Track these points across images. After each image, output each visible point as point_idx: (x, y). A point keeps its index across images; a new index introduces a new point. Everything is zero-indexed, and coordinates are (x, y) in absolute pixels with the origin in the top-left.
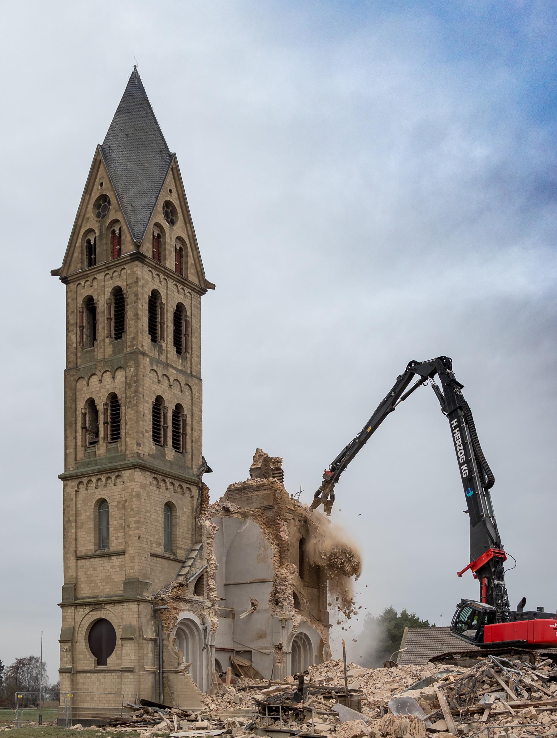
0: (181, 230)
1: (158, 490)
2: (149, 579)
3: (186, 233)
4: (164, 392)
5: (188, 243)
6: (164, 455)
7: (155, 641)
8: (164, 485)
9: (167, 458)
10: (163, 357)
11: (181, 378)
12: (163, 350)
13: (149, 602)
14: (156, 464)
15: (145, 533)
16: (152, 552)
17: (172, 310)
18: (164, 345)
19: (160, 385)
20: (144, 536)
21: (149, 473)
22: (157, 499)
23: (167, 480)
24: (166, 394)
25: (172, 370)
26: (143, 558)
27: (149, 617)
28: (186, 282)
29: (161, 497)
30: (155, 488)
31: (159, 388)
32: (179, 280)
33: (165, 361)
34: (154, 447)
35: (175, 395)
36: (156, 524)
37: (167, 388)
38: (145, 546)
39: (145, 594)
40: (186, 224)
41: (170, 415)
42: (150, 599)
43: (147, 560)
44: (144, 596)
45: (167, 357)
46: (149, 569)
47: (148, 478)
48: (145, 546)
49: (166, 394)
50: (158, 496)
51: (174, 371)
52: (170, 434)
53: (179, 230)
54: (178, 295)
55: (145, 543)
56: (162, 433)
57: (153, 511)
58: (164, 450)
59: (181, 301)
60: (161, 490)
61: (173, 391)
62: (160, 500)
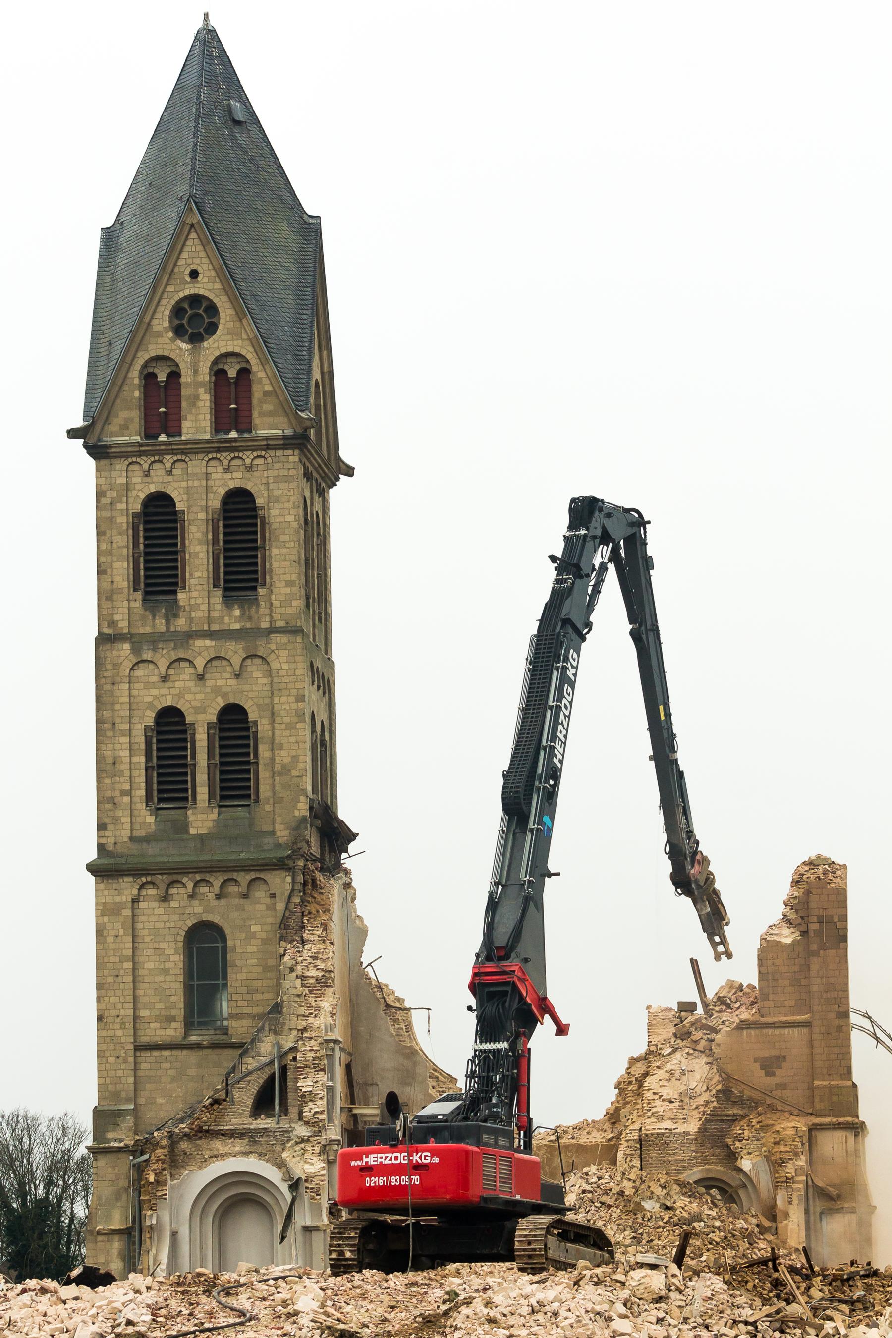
0: (229, 337)
1: (166, 904)
2: (128, 1100)
3: (244, 336)
4: (180, 696)
5: (249, 356)
6: (182, 827)
7: (126, 1233)
8: (182, 891)
9: (193, 831)
10: (181, 624)
11: (235, 651)
12: (179, 607)
13: (119, 1150)
14: (154, 853)
15: (119, 1006)
16: (144, 1040)
17: (202, 516)
18: (181, 596)
19: (167, 685)
20: (114, 1013)
21: (131, 879)
22: (158, 925)
23: (185, 880)
24: (188, 697)
25: (199, 643)
26: (112, 1060)
27: (123, 1183)
28: (238, 444)
29: (176, 917)
30: (155, 904)
31: (165, 691)
32: (219, 448)
33: (186, 629)
34: (151, 819)
35: (217, 691)
36: (161, 978)
37: (191, 684)
38: (119, 1033)
39: (110, 1135)
40: (241, 320)
41: (201, 738)
42: (122, 1144)
43: (125, 1061)
44: (109, 1141)
45: (191, 620)
46: (131, 1080)
47: (128, 888)
48: (119, 1033)
49: (188, 697)
50: (165, 918)
51: (208, 643)
52: (202, 777)
53: (229, 338)
54: (228, 476)
55: (118, 1026)
56: (189, 778)
57: (150, 952)
58: (186, 817)
59: (232, 485)
60: (173, 904)
61: (209, 683)
62: (172, 924)
